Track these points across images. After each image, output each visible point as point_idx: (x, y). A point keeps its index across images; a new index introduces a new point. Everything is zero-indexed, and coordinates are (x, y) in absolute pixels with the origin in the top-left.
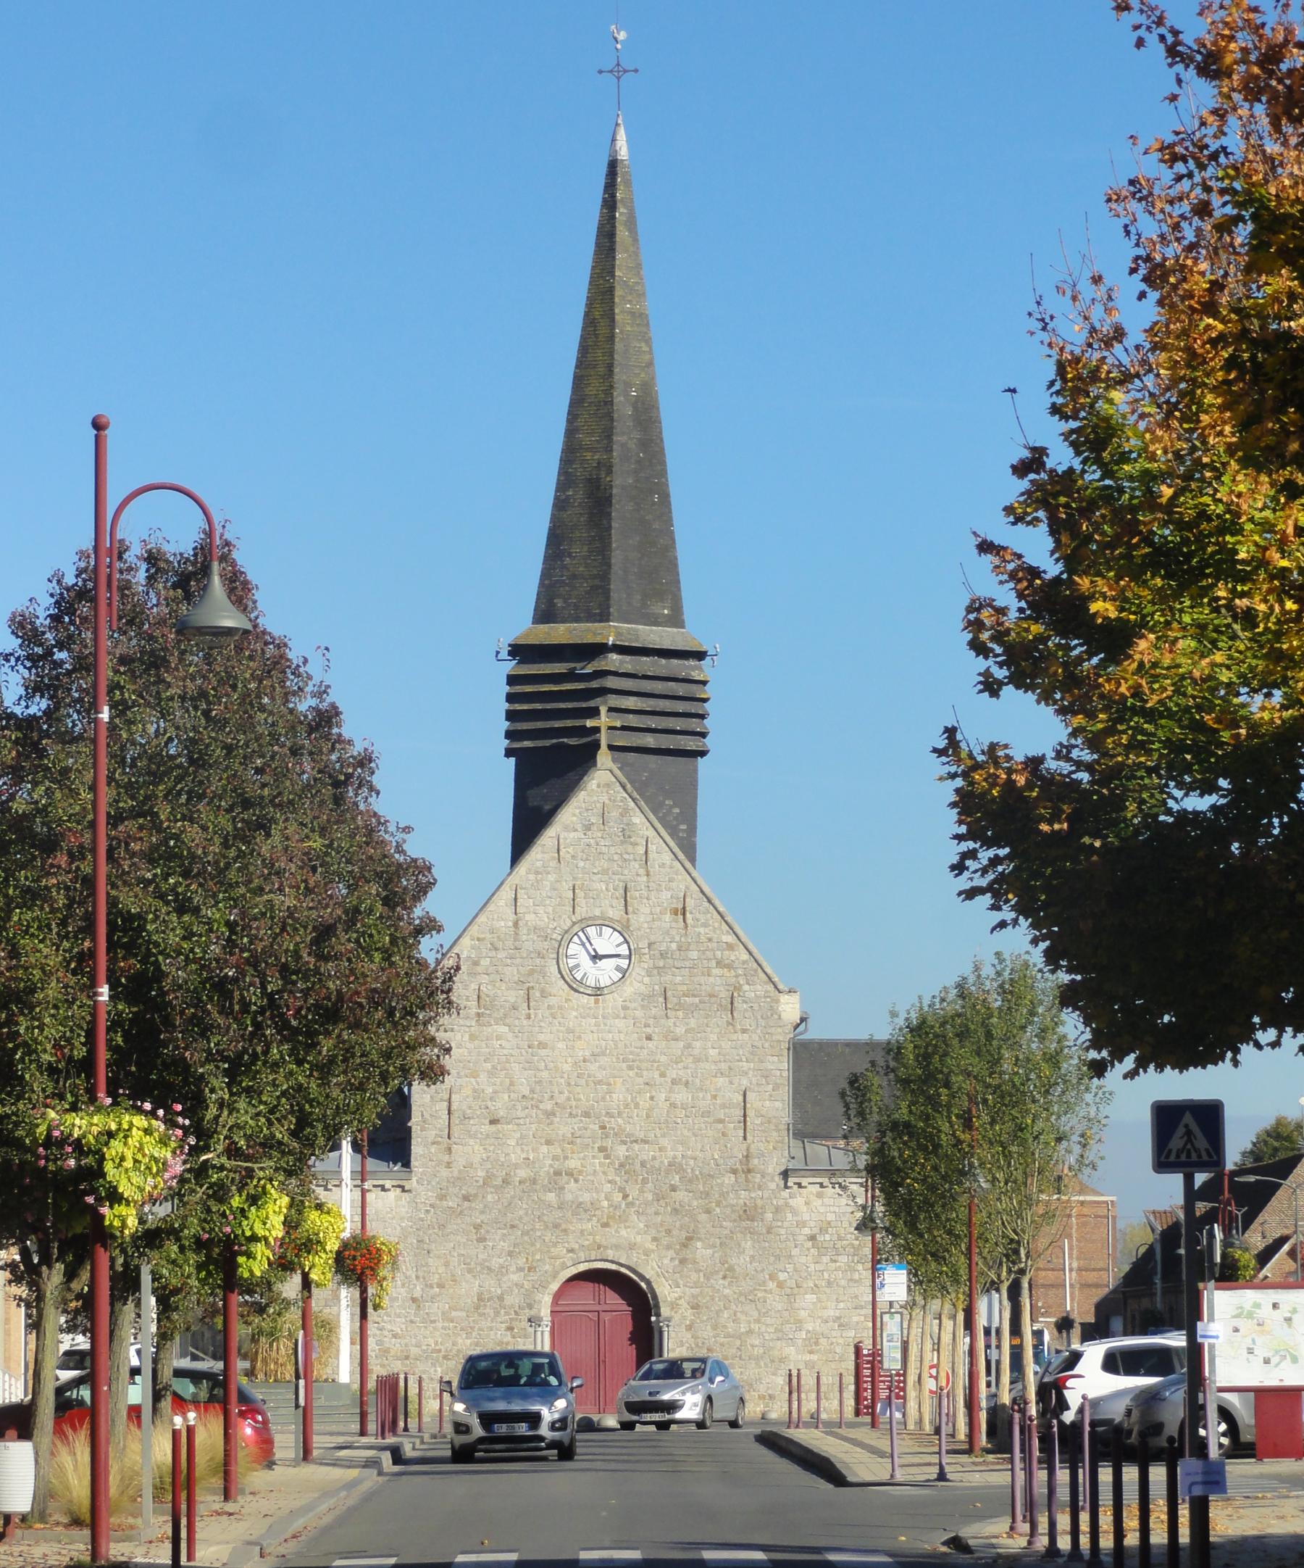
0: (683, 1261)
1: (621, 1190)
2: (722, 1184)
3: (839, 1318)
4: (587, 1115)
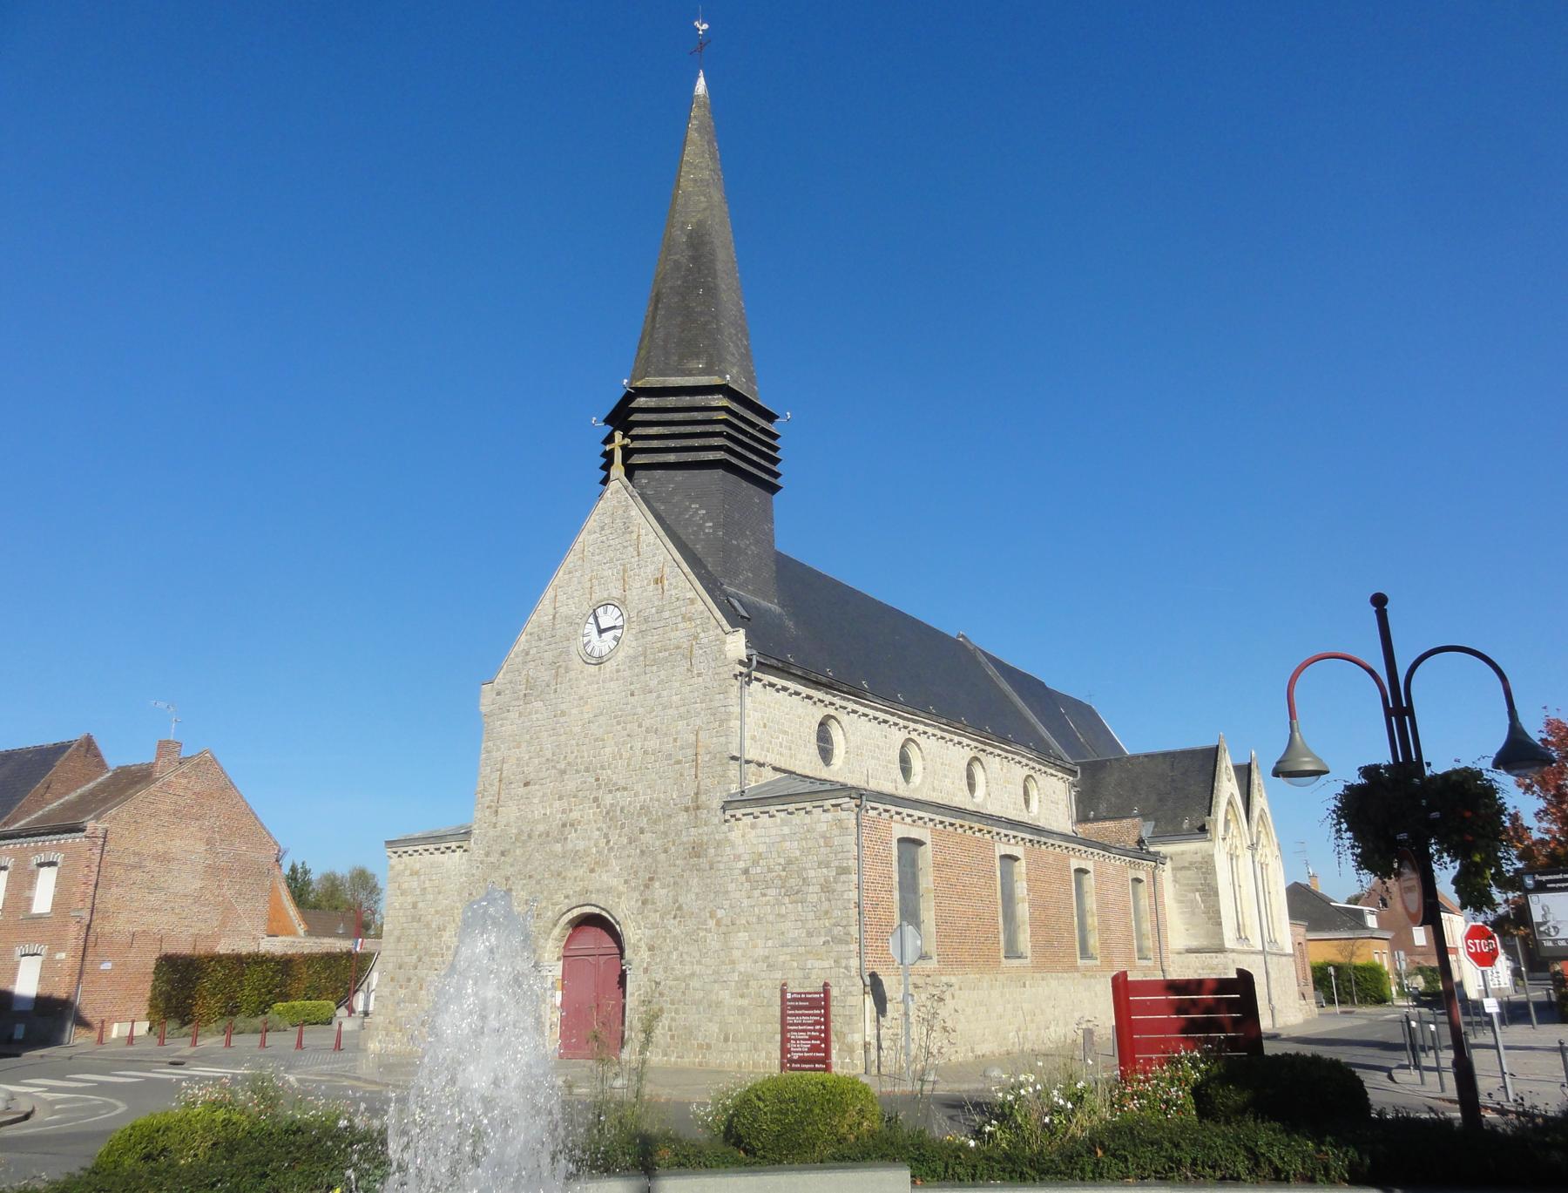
0: (644, 903)
1: (606, 836)
2: (676, 824)
4: (587, 770)
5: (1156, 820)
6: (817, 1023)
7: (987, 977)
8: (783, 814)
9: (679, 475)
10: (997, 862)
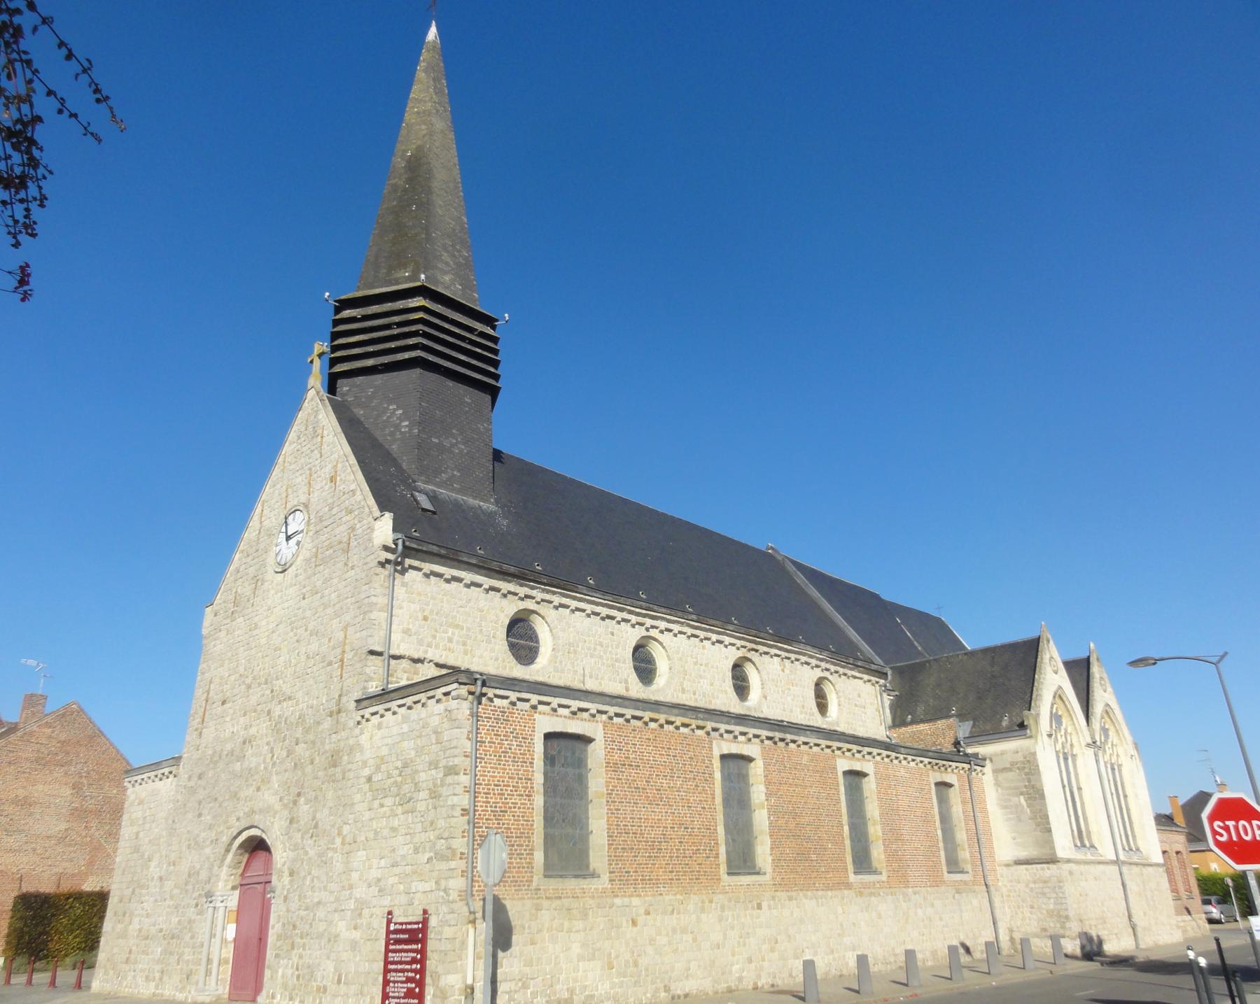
3: (379, 880)
5: (975, 720)
6: (414, 961)
7: (695, 898)
8: (403, 710)
9: (378, 379)
10: (717, 764)
